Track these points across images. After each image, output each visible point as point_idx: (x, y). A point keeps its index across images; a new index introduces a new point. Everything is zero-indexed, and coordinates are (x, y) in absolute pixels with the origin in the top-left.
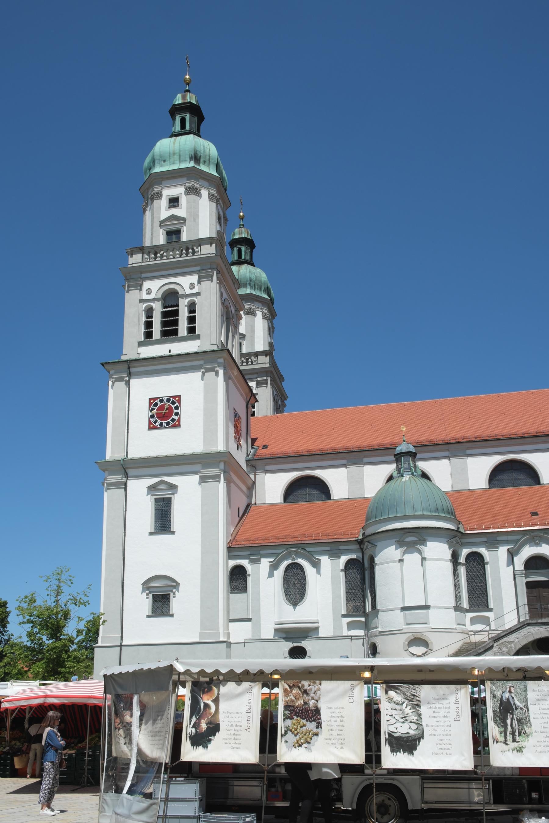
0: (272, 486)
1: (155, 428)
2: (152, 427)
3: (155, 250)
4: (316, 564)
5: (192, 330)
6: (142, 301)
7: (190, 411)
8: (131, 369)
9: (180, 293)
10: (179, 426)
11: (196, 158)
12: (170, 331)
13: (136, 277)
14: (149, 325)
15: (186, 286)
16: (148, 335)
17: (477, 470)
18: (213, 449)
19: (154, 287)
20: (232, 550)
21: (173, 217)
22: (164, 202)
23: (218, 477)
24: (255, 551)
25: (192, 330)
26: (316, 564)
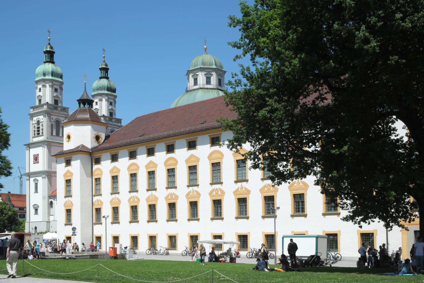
2: (34, 163)
5: (42, 133)
6: (33, 124)
7: (40, 159)
8: (29, 146)
10: (38, 163)
11: (44, 75)
13: (32, 116)
16: (35, 134)
18: (44, 170)
19: (35, 119)
21: (39, 96)
22: (38, 90)
23: (45, 177)
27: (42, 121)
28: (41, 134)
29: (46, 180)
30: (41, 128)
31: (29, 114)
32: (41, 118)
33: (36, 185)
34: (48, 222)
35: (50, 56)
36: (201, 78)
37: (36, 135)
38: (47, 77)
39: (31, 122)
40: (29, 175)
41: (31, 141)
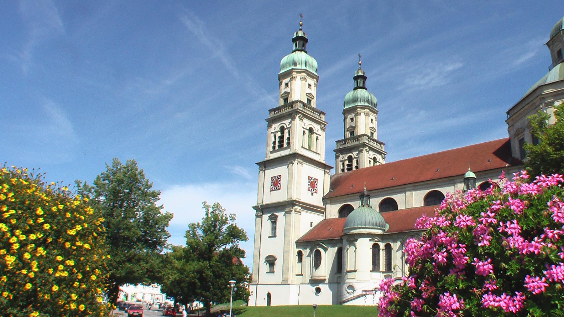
1: (273, 190)
5: (288, 144)
7: (283, 182)
9: (285, 127)
10: (279, 189)
13: (271, 122)
14: (274, 143)
15: (287, 124)
16: (274, 147)
19: (276, 127)
25: (288, 144)
27: (288, 126)
28: (285, 145)
30: (286, 136)
31: (267, 120)
33: (274, 223)
37: (277, 148)
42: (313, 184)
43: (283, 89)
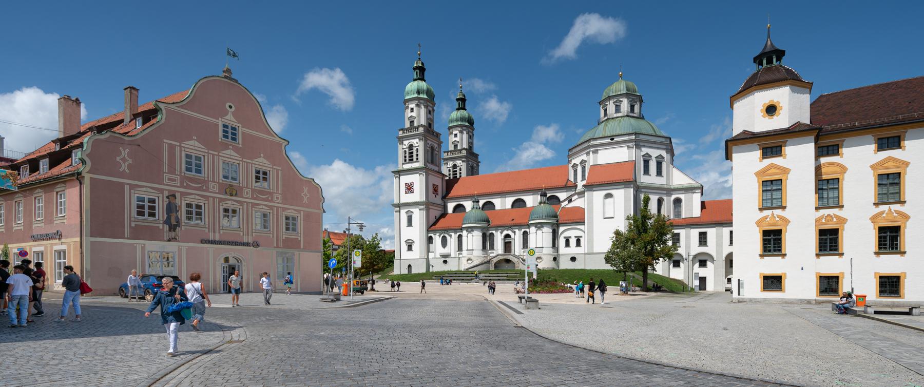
0: (451, 206)
3: (407, 129)
4: (451, 236)
7: (416, 188)
8: (399, 173)
11: (418, 92)
12: (411, 160)
13: (401, 140)
17: (509, 201)
19: (406, 143)
20: (428, 231)
24: (435, 231)
26: (451, 236)
29: (424, 213)
32: (415, 142)
34: (428, 260)
35: (421, 73)
36: (625, 105)
38: (421, 96)
39: (400, 146)
40: (400, 206)
41: (400, 168)
42: (435, 189)
43: (409, 114)
